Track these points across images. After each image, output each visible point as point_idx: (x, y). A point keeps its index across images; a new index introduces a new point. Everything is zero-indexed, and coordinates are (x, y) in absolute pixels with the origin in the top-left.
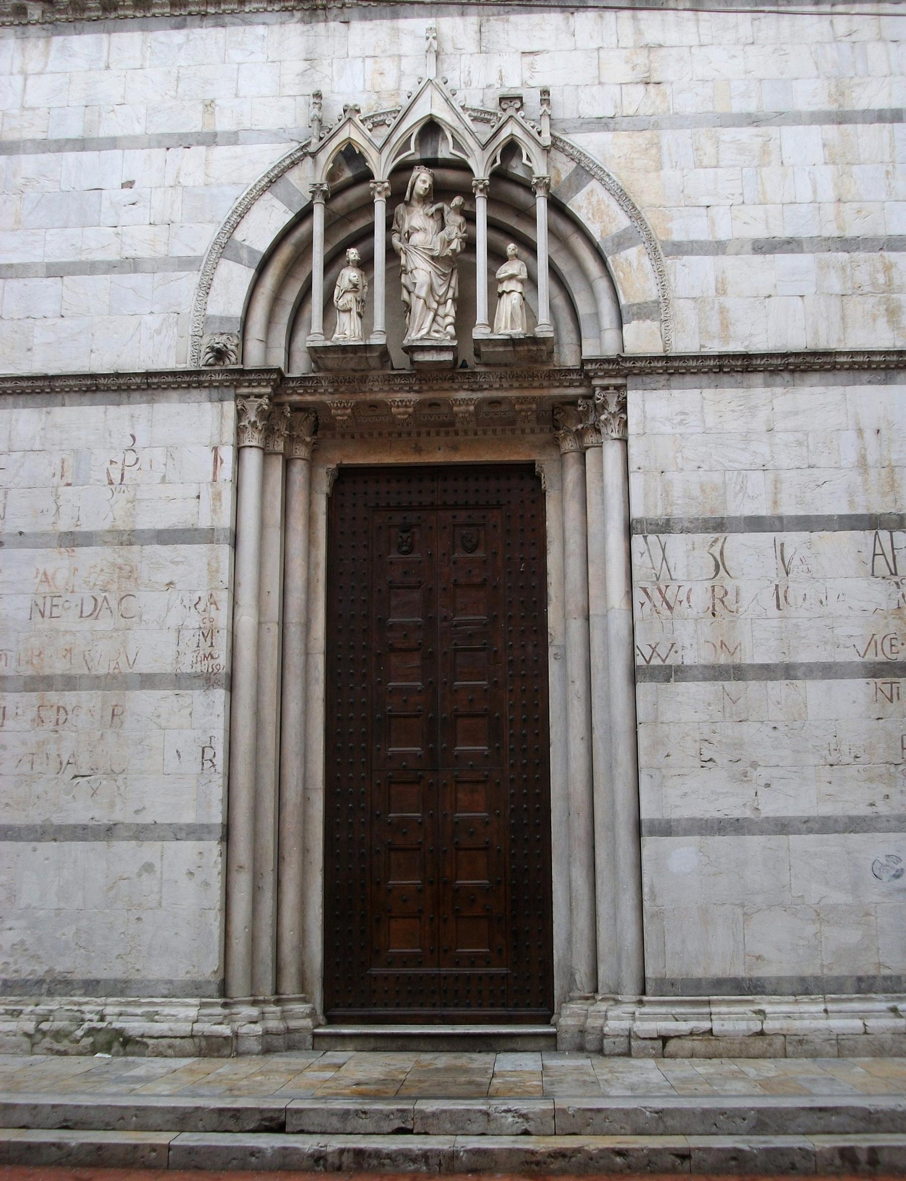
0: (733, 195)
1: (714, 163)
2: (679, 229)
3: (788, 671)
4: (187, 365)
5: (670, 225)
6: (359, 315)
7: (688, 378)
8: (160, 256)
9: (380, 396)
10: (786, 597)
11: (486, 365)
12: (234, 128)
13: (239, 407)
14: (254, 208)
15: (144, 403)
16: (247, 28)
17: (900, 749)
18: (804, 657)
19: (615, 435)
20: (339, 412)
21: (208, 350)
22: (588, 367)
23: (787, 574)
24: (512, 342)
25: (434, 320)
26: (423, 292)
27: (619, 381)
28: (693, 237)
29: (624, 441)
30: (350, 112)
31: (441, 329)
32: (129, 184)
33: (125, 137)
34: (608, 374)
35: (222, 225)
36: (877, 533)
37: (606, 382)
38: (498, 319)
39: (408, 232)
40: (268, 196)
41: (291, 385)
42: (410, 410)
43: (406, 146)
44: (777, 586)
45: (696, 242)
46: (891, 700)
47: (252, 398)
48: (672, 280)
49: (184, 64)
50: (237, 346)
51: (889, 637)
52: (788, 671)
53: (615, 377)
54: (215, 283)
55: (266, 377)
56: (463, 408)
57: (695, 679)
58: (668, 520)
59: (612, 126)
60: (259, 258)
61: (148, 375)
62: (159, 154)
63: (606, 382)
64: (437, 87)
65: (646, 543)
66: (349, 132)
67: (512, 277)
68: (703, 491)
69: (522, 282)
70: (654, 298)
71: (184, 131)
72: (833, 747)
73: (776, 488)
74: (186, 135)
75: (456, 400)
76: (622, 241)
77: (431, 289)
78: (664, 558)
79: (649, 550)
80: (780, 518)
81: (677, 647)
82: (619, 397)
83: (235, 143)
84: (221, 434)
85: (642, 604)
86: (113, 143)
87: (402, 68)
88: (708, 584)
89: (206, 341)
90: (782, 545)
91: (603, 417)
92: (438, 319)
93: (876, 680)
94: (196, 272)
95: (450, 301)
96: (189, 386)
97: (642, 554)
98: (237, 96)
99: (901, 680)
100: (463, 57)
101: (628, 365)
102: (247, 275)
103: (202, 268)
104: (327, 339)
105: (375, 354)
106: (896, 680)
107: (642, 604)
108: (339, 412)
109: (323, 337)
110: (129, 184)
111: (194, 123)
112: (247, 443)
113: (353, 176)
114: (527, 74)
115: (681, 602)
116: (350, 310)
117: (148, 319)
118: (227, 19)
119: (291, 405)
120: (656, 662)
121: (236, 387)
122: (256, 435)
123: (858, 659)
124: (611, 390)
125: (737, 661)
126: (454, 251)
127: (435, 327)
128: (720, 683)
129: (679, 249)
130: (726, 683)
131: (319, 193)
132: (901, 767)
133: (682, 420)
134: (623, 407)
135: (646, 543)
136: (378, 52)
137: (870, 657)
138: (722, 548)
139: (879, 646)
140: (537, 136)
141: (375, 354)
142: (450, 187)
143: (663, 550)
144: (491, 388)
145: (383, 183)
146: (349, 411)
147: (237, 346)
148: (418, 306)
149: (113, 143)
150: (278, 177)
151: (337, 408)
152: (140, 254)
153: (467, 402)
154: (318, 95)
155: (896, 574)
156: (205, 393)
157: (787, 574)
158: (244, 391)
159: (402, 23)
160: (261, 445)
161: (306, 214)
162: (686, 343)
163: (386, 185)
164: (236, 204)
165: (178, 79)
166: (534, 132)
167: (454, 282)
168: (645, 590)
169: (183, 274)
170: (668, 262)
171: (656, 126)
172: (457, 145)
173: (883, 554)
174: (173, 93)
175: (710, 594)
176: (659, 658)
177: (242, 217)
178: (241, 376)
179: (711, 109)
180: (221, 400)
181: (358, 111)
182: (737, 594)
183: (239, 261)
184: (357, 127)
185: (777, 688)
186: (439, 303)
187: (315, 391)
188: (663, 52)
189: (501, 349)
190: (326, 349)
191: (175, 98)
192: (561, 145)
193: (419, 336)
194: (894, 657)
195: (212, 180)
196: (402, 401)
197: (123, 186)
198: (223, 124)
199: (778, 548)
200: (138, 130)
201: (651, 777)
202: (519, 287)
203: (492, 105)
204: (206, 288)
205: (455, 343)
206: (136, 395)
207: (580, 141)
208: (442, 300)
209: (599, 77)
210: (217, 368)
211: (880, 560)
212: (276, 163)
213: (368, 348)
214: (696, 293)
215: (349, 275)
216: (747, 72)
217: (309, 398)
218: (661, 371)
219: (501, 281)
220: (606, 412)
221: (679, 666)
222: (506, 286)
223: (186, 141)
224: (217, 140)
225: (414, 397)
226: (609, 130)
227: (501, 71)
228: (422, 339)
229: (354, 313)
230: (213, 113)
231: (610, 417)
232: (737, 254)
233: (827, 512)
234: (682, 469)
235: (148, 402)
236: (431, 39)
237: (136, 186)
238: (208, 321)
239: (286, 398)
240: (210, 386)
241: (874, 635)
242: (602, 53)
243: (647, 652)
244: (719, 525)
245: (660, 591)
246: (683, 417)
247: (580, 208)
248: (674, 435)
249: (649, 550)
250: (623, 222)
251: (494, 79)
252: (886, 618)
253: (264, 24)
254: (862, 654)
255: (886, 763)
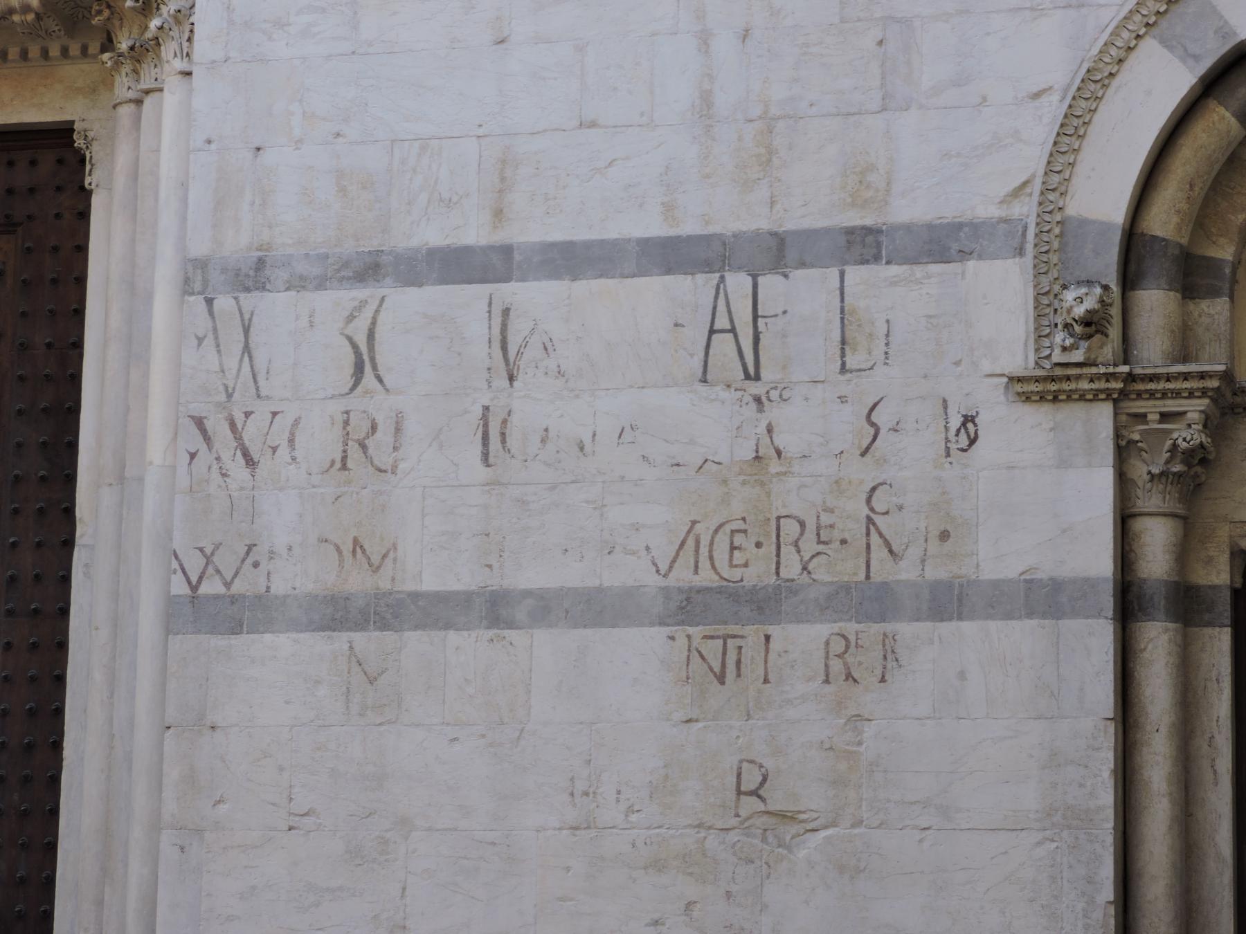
3: (495, 609)
10: (503, 434)
17: (731, 795)
18: (532, 576)
23: (511, 378)
36: (722, 277)
44: (486, 408)
46: (721, 679)
51: (728, 528)
52: (495, 609)
57: (295, 626)
58: (260, 264)
65: (211, 313)
68: (343, 190)
72: (580, 786)
73: (503, 179)
78: (247, 349)
79: (215, 330)
80: (506, 251)
81: (260, 553)
85: (193, 456)
88: (336, 408)
90: (506, 312)
93: (691, 630)
97: (200, 340)
99: (748, 630)
106: (733, 629)
107: (193, 456)
115: (274, 449)
120: (211, 587)
123: (652, 580)
125: (385, 585)
128: (345, 636)
130: (358, 637)
132: (733, 837)
135: (211, 313)
137: (683, 576)
138: (374, 323)
139: (704, 550)
143: (246, 331)
155: (757, 378)
157: (511, 378)
168: (199, 423)
173: (733, 330)
175: (338, 431)
176: (217, 577)
182: (398, 430)
185: (466, 649)
194: (736, 574)
199: (497, 321)
201: (182, 849)
211: (724, 344)
221: (259, 597)
233: (612, 232)
234: (299, 141)
241: (694, 523)
243: (194, 565)
244: (368, 269)
245: (233, 425)
249: (215, 330)
252: (725, 482)
254: (663, 567)
255: (699, 826)
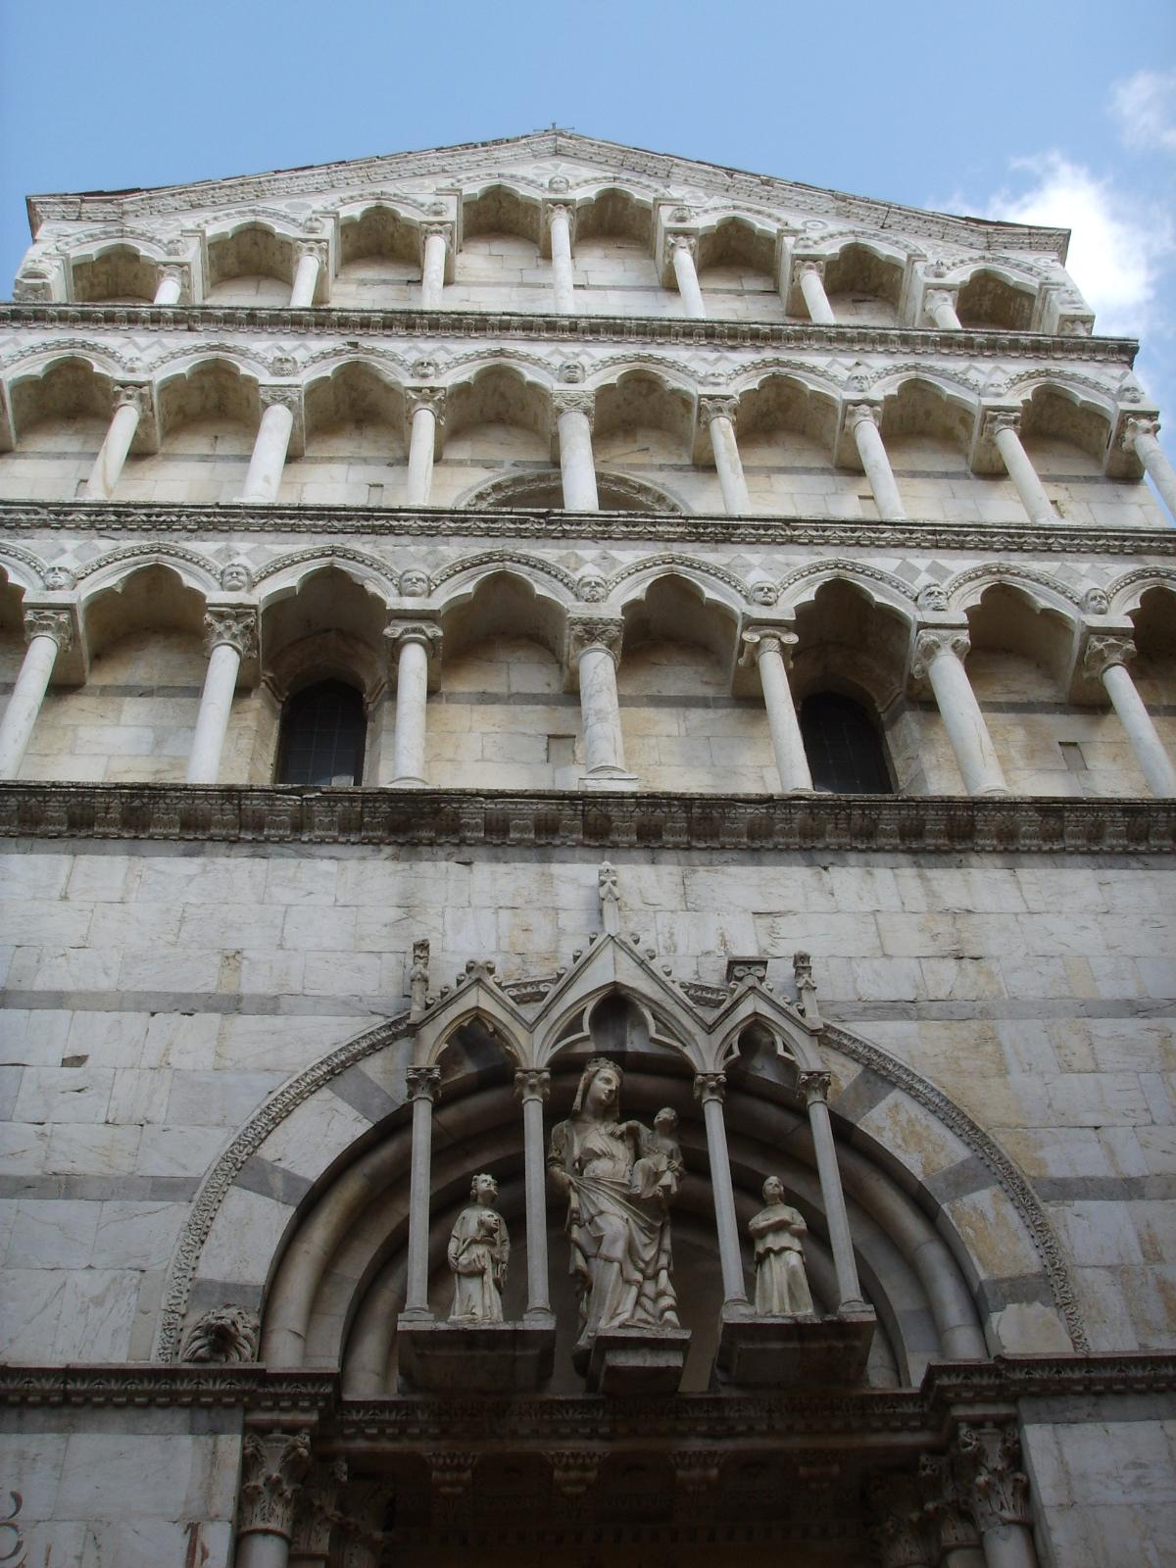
0: (1133, 1111)
1: (1091, 1065)
2: (1062, 1157)
4: (155, 1361)
5: (1040, 1154)
6: (497, 1283)
7: (1132, 1403)
8: (117, 1174)
9: (531, 1446)
11: (741, 1385)
12: (273, 991)
13: (248, 1451)
14: (298, 1112)
15: (51, 1430)
16: (304, 861)
19: (1007, 1514)
20: (448, 1476)
21: (197, 1333)
22: (945, 1381)
24: (796, 1330)
25: (637, 1303)
26: (618, 1251)
27: (1003, 1410)
28: (1085, 1171)
29: (1030, 1528)
30: (477, 973)
31: (650, 1319)
32: (78, 1061)
33: (80, 993)
34: (980, 1397)
35: (240, 1131)
37: (978, 1411)
38: (764, 1291)
39: (580, 1160)
40: (326, 1093)
41: (354, 1416)
42: (592, 1475)
43: (574, 1026)
45: (1091, 1180)
47: (277, 1434)
48: (1063, 1237)
49: (193, 900)
50: (255, 1329)
53: (993, 1401)
54: (217, 1226)
55: (310, 1389)
56: (696, 1473)
59: (913, 1013)
60: (304, 1190)
61: (69, 1373)
62: (136, 1021)
63: (978, 1411)
64: (622, 945)
66: (475, 998)
67: (780, 1227)
69: (798, 1234)
70: (1036, 1268)
71: (186, 990)
74: (187, 996)
75: (683, 1455)
76: (962, 1180)
77: (631, 1250)
82: (1004, 1441)
83: (274, 1012)
84: (208, 1496)
86: (58, 1000)
87: (560, 925)
89: (195, 1318)
91: (981, 1479)
92: (644, 1300)
94: (185, 1203)
95: (664, 1274)
96: (151, 1403)
98: (281, 947)
100: (659, 916)
101: (1019, 1375)
102: (281, 1216)
103: (197, 1197)
104: (438, 1319)
105: (532, 1352)
108: (448, 1476)
109: (431, 1316)
110: (78, 1061)
111: (207, 979)
112: (259, 1524)
113: (479, 1073)
114: (766, 942)
116: (481, 1273)
117: (82, 1278)
118: (271, 848)
119: (350, 1457)
121: (247, 1410)
122: (279, 1510)
124: (989, 1428)
126: (666, 1188)
127: (640, 1314)
129: (1066, 1190)
131: (423, 1083)
133: (1139, 1478)
134: (1016, 1458)
136: (519, 902)
140: (798, 1016)
141: (532, 1352)
142: (656, 1092)
144: (751, 1431)
145: (539, 1072)
146: (467, 1475)
147: (255, 1329)
148: (608, 1276)
149: (58, 1000)
150: (344, 1065)
151: (444, 1468)
152: (80, 1168)
153: (704, 1459)
154: (423, 946)
156: (181, 1417)
158: (261, 1417)
159: (556, 869)
160: (285, 1531)
161: (395, 1125)
162: (1113, 1339)
163: (546, 1075)
164: (269, 1101)
165: (182, 920)
166: (793, 1010)
167: (667, 1243)
169: (159, 1205)
170: (1050, 1210)
171: (986, 1014)
172: (665, 1027)
174: (171, 938)
177: (276, 1121)
178: (257, 1390)
179: (1068, 994)
180: (215, 1432)
181: (491, 971)
183: (265, 1190)
184: (490, 992)
186: (646, 1278)
187: (403, 1432)
188: (975, 919)
189: (777, 1345)
190: (434, 1338)
191: (173, 945)
192: (834, 1037)
193: (616, 1322)
195: (229, 1063)
196: (575, 1456)
197: (65, 1063)
198: (255, 983)
200: (104, 984)
202: (797, 1245)
203: (713, 978)
204: (200, 1232)
205: (686, 1335)
206: (38, 1417)
207: (867, 1031)
208: (650, 1271)
209: (882, 946)
210: (212, 1366)
212: (344, 1044)
213: (518, 1337)
214: (1110, 1259)
215: (473, 1219)
216: (1109, 947)
217: (388, 1446)
218: (1080, 1388)
219: (762, 1233)
220: (984, 1471)
222: (772, 1241)
223: (187, 1005)
224: (242, 1005)
225: (598, 1447)
226: (911, 1019)
227: (722, 935)
228: (623, 1326)
229: (489, 1278)
230: (237, 969)
231: (994, 1479)
232: (1164, 1198)
235: (60, 1430)
236: (609, 884)
237: (89, 1062)
238: (200, 1290)
239: (340, 1444)
240: (195, 1403)
242: (880, 918)
246: (1139, 1472)
247: (880, 1130)
248: (1130, 1506)
250: (956, 1151)
251: (712, 943)
253: (331, 858)
